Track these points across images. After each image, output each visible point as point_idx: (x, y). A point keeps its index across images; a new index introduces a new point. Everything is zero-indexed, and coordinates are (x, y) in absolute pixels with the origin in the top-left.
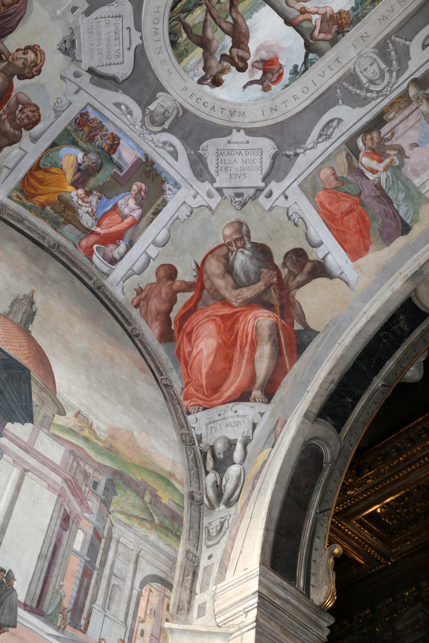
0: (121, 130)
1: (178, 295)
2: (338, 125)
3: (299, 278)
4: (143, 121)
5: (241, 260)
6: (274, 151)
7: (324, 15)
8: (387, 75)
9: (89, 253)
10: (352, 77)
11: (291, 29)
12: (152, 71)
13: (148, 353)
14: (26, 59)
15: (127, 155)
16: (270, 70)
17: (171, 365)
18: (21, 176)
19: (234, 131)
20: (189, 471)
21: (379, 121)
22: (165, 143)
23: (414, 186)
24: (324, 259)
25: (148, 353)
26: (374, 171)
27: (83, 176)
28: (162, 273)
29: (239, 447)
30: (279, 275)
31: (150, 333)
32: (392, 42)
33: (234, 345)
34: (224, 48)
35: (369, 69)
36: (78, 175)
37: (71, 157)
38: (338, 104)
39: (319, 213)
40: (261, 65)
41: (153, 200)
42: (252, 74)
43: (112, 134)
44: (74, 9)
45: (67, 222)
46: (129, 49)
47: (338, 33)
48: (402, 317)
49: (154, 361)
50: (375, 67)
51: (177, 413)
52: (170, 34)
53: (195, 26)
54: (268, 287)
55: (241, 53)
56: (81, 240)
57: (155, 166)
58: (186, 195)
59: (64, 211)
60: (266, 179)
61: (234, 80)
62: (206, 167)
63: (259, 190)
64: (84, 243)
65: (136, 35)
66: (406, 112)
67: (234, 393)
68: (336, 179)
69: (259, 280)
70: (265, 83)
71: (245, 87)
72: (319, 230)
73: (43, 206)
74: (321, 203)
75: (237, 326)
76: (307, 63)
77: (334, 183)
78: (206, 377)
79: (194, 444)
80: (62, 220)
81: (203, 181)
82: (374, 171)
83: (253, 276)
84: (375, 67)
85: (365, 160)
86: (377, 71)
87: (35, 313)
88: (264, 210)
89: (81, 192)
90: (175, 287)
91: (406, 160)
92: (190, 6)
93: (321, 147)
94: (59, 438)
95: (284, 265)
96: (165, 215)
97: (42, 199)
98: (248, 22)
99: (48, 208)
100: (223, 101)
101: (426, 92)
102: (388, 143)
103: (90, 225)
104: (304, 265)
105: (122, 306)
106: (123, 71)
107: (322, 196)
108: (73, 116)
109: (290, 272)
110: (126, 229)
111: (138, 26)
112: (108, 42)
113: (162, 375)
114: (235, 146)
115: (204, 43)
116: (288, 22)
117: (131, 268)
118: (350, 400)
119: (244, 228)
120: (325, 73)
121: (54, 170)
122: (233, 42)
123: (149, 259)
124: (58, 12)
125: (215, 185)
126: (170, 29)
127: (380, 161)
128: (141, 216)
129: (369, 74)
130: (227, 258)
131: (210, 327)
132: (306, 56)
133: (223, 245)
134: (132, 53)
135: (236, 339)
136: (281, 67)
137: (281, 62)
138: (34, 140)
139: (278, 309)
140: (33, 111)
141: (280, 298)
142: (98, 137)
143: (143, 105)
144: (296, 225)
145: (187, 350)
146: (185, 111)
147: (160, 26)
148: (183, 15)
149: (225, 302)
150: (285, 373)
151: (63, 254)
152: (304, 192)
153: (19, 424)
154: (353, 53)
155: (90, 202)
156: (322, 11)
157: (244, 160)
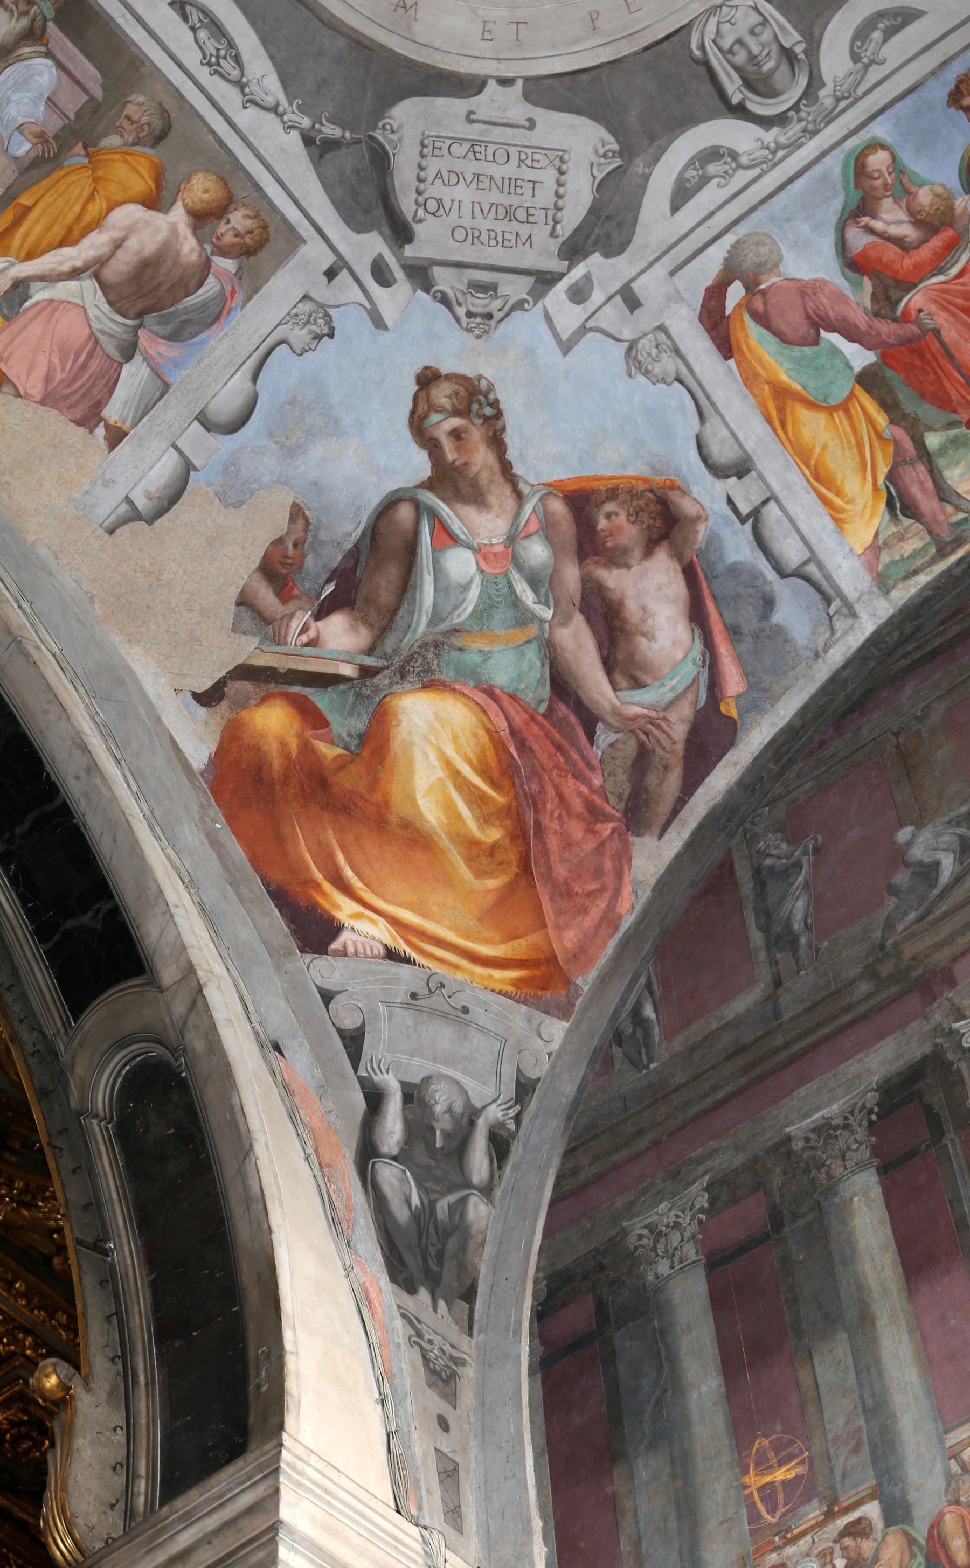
101: (51, 25)
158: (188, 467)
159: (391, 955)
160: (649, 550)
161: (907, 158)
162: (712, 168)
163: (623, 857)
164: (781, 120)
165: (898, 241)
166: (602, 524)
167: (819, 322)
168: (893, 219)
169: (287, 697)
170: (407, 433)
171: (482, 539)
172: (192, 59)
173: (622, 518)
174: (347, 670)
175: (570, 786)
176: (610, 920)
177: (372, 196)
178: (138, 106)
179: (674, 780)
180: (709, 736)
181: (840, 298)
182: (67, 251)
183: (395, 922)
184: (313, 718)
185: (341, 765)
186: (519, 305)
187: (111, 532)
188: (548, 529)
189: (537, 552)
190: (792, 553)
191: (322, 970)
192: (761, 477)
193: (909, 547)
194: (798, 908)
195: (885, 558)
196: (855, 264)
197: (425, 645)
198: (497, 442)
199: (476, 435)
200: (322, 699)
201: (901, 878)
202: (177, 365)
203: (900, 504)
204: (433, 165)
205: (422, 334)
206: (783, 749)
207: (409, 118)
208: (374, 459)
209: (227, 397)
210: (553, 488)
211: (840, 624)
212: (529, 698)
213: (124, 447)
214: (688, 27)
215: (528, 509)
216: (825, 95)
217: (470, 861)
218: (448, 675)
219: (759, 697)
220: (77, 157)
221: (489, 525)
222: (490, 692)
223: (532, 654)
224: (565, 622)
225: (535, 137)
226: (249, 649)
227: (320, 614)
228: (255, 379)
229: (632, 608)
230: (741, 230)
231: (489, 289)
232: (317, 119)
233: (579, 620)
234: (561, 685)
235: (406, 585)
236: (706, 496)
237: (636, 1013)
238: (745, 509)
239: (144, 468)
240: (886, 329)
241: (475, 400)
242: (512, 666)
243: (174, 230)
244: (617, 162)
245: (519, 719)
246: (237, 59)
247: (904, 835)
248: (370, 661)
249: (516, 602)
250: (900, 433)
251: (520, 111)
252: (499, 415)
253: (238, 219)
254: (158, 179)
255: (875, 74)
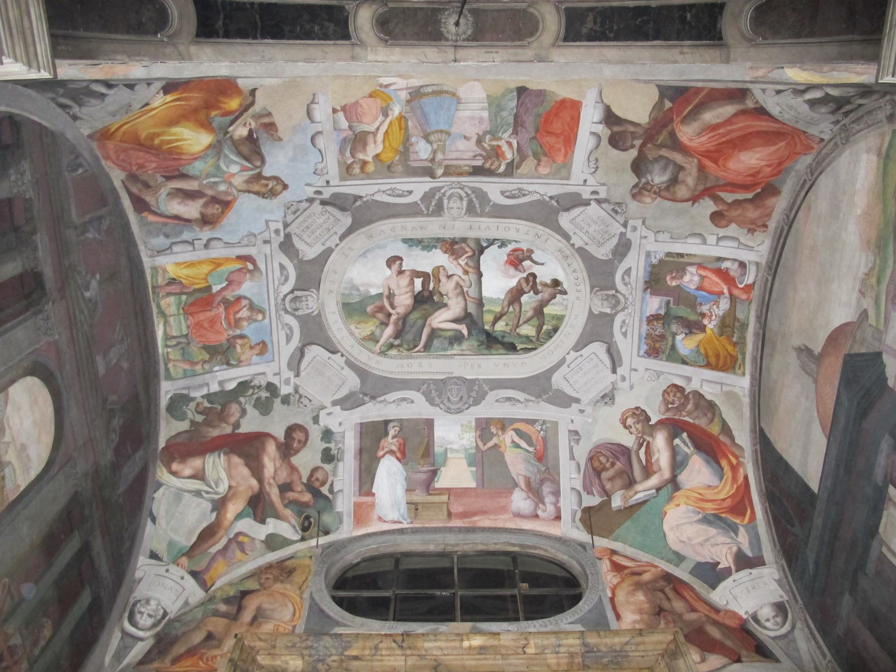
0: (641, 320)
1: (729, 201)
2: (506, 192)
3: (631, 129)
4: (623, 310)
5: (659, 178)
6: (564, 213)
7: (456, 259)
8: (448, 194)
9: (749, 288)
10: (471, 210)
11: (482, 269)
12: (584, 328)
13: (795, 201)
14: (634, 423)
15: (655, 304)
16: (517, 260)
17: (793, 173)
18: (721, 374)
19: (576, 247)
20: (869, 126)
21: (477, 171)
22: (626, 284)
23: (490, 113)
24: (601, 123)
25: (795, 201)
26: (510, 144)
27: (693, 327)
28: (723, 222)
29: (809, 96)
30: (643, 145)
31: (780, 204)
32: (428, 210)
33: (728, 142)
34: (531, 297)
35: (454, 207)
36: (694, 331)
37: (685, 344)
38: (494, 204)
39: (573, 152)
40: (520, 267)
41: (676, 264)
42: (530, 267)
43: (648, 324)
44: (582, 411)
45: (735, 319)
46: (582, 356)
47: (457, 243)
48: (584, 31)
49: (798, 195)
50: (451, 205)
51: (827, 155)
52: (551, 337)
53: (533, 326)
54: (661, 146)
55: (524, 285)
56: (743, 300)
57: (647, 279)
58: (648, 247)
59: (728, 326)
60: (587, 203)
61: (544, 275)
62: (617, 246)
63: (599, 202)
64: (744, 297)
65: (569, 359)
66: (454, 163)
67: (767, 121)
68: (539, 161)
69: (661, 157)
70: (528, 255)
71: (542, 264)
72: (584, 142)
73: (735, 344)
74: (565, 156)
75: (711, 148)
76: (491, 242)
77: (544, 159)
78: (776, 144)
79: (844, 125)
80: (737, 324)
81: (629, 240)
82: (510, 144)
83: (662, 163)
84: (451, 205)
85: (509, 156)
86: (452, 202)
87: (806, 347)
88: (608, 189)
89: (705, 322)
90: (726, 207)
91: (481, 133)
92: (524, 340)
93: (531, 188)
94: (885, 318)
95: (633, 146)
96: (678, 248)
97: (730, 348)
98: (502, 297)
99: (734, 339)
100: (564, 269)
102: (484, 154)
103: (726, 300)
104: (619, 133)
105: (774, 237)
106: (598, 349)
107: (560, 159)
108: (655, 361)
109: (634, 138)
110: (710, 270)
111: (564, 360)
112: (586, 372)
113: (805, 180)
114: (585, 238)
115: (539, 313)
116: (480, 275)
117: (738, 248)
118: (689, 16)
119: (634, 191)
120: (485, 227)
121: (702, 351)
122: (522, 295)
123: (719, 239)
124: (590, 420)
125: (623, 230)
126: (547, 340)
127: (499, 147)
128: (692, 264)
129: (458, 204)
130: (667, 188)
131: (732, 165)
132: (487, 247)
133: (660, 196)
134: (583, 352)
135: (723, 143)
136: (509, 255)
137: (506, 258)
138: (689, 379)
139: (669, 128)
140: (668, 394)
141: (659, 132)
142: (657, 333)
143: (611, 318)
144: (597, 160)
145: (768, 170)
146: (592, 288)
147: (552, 348)
148: (534, 339)
149: (701, 168)
150: (712, 90)
151: (761, 312)
152: (569, 174)
153: (886, 370)
154: (458, 224)
155: (709, 310)
156: (455, 262)
157: (588, 225)
158: (313, 122)
159: (147, 104)
160: (202, 214)
161: (257, 324)
162: (283, 278)
163: (123, 169)
164: (284, 299)
165: (238, 312)
166: (217, 206)
167: (230, 283)
168: (244, 313)
169: (237, 110)
170: (276, 175)
171: (236, 177)
172: (398, 186)
173: (215, 211)
174: (231, 129)
175: (154, 165)
176: (108, 157)
177: (338, 202)
178: (399, 168)
179: (135, 190)
180: (140, 205)
181: (233, 291)
182: (384, 131)
183: (155, 109)
184: (226, 114)
185: (208, 115)
186: (285, 217)
187: (314, 95)
188: (226, 193)
189: (222, 188)
190: (176, 248)
191: (158, 85)
192: (201, 250)
193: (160, 279)
194: (90, 235)
195: (160, 272)
196: (239, 299)
197: (221, 150)
198: (257, 193)
199: (263, 190)
200: (228, 119)
201: (89, 276)
202: (338, 135)
203: (173, 281)
204: (332, 219)
205: (298, 191)
206: (126, 226)
207: (346, 220)
208: (277, 162)
209: (320, 142)
210: (235, 199)
211: (150, 253)
212: (187, 167)
213: (331, 111)
214: (318, 291)
215: (235, 191)
216: (283, 313)
217: (155, 133)
218: (209, 152)
219: (143, 223)
220: (401, 148)
221: (238, 181)
222: (196, 159)
223: (197, 173)
224: (199, 185)
225: (320, 243)
226: (257, 108)
227: (251, 132)
228: (320, 151)
229: (190, 202)
230: (264, 276)
231: (294, 213)
232: (364, 202)
233: (197, 189)
234: (184, 176)
235: (240, 154)
236: (206, 234)
237: (80, 165)
238: (196, 242)
239: (322, 112)
240: (219, 299)
241: (273, 194)
242: (198, 167)
243: (367, 156)
244: (300, 257)
245: (183, 162)
246: (390, 195)
247: (98, 276)
248: (228, 135)
249: (214, 176)
250: (191, 290)
251: (329, 244)
252: (263, 197)
253: (357, 170)
254: (380, 161)
255: (280, 326)
